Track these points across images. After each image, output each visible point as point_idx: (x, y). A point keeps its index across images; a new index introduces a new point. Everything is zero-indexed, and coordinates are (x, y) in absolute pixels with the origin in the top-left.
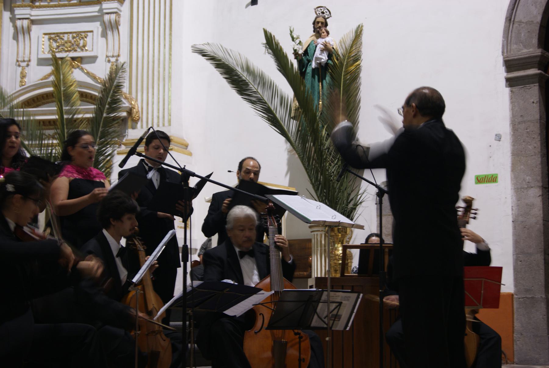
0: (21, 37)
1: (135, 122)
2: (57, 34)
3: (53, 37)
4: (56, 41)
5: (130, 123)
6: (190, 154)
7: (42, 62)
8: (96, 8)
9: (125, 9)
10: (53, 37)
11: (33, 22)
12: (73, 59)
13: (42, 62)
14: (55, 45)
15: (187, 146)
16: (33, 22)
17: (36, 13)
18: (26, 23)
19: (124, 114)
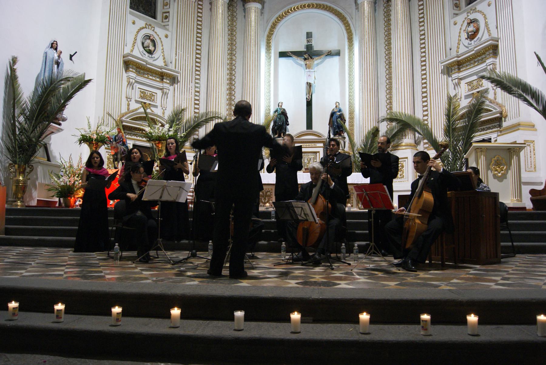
0: (456, 88)
1: (505, 118)
2: (470, 82)
3: (469, 84)
4: (470, 85)
5: (503, 119)
6: (536, 130)
7: (467, 97)
8: (485, 64)
9: (497, 60)
10: (469, 84)
11: (461, 79)
12: (478, 92)
13: (467, 97)
14: (470, 87)
15: (534, 126)
16: (461, 79)
17: (461, 75)
18: (456, 80)
19: (498, 115)
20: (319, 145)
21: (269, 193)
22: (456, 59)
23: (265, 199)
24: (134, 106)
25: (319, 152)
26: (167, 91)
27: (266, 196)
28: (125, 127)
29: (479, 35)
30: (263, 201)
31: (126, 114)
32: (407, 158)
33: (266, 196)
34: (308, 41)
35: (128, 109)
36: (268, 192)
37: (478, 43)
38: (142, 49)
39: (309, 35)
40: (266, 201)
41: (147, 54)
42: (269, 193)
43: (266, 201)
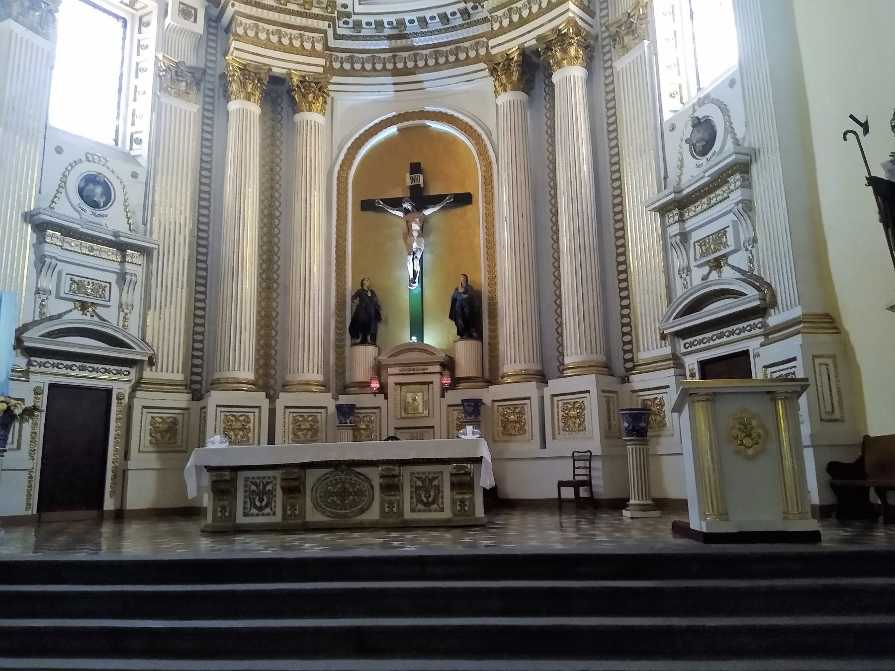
20: (431, 369)
21: (269, 487)
22: (672, 196)
23: (261, 501)
24: (55, 307)
25: (432, 383)
26: (134, 278)
27: (264, 492)
28: (30, 352)
29: (716, 147)
30: (258, 504)
31: (35, 323)
32: (588, 392)
33: (264, 492)
34: (413, 179)
35: (41, 314)
36: (268, 483)
37: (715, 160)
38: (77, 200)
39: (415, 168)
40: (264, 503)
41: (89, 210)
42: (269, 487)
43: (264, 503)
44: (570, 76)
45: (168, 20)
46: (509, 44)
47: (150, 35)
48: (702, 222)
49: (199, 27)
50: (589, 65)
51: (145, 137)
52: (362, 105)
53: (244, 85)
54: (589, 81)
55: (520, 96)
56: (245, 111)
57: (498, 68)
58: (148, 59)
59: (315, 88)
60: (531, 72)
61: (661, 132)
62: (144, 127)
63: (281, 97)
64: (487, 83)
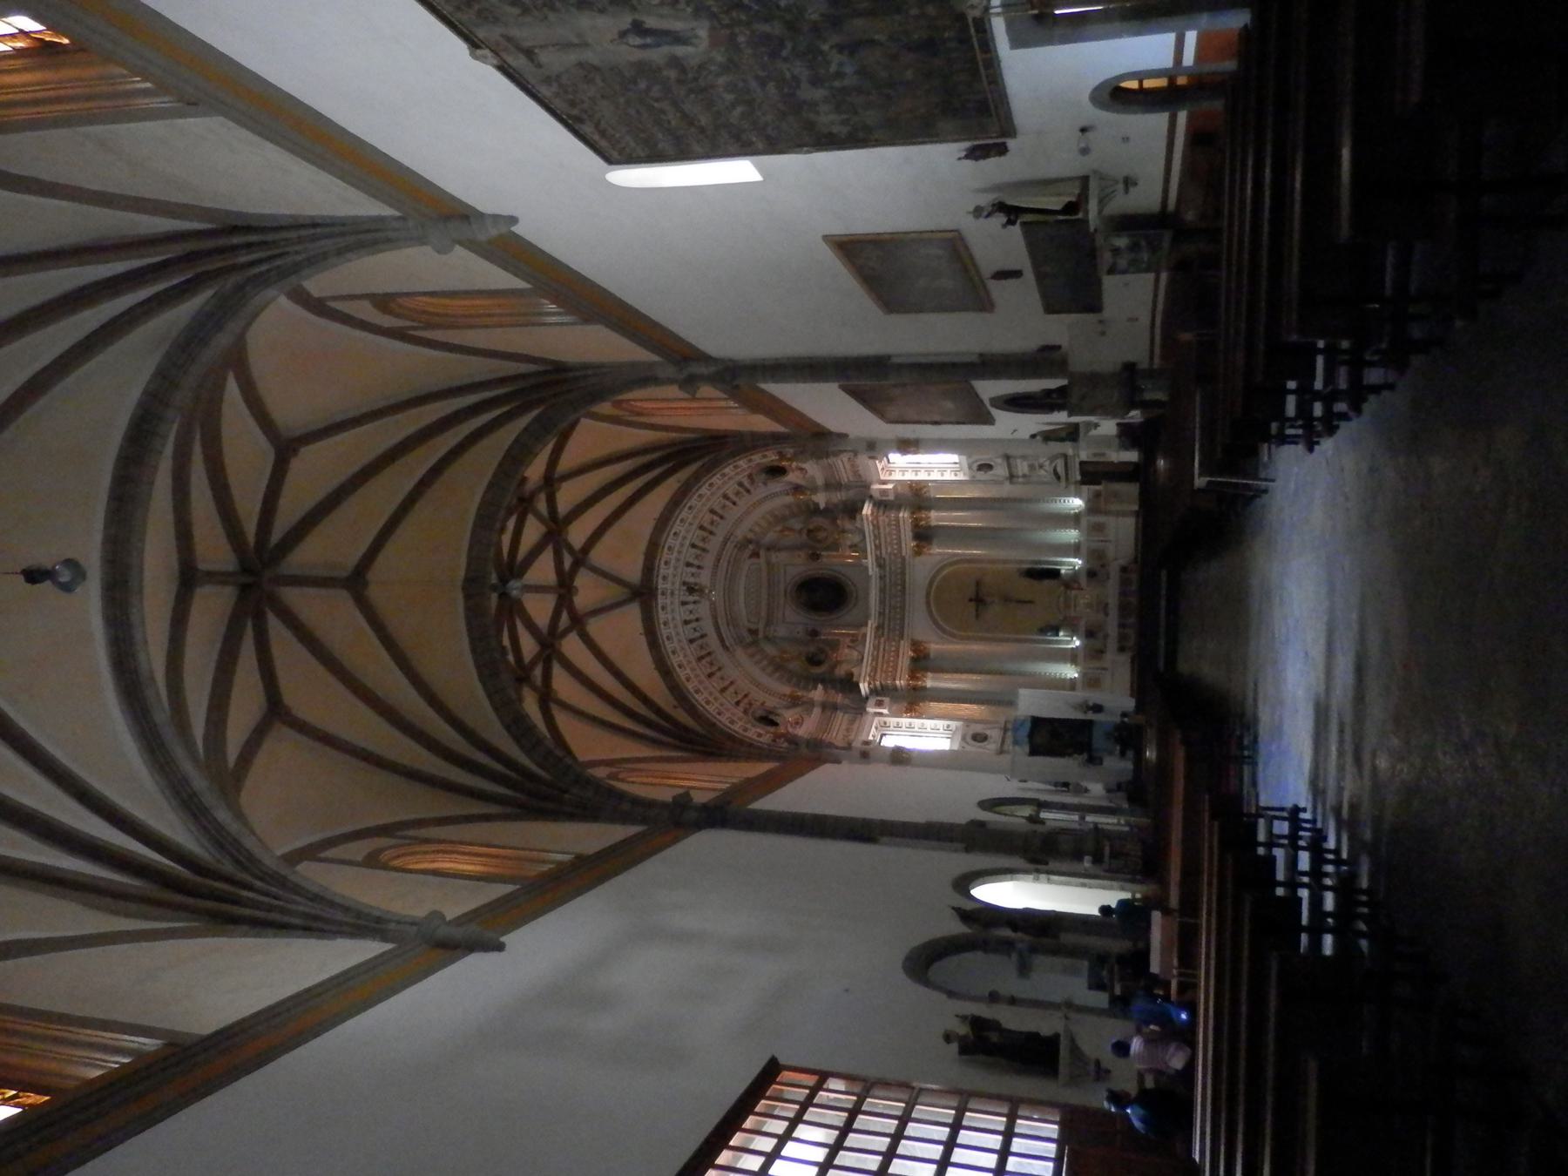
44: (936, 517)
45: (885, 711)
46: (909, 543)
47: (893, 721)
48: (1022, 467)
49: (887, 700)
50: (929, 509)
51: (947, 723)
52: (920, 626)
53: (918, 679)
54: (939, 509)
55: (935, 541)
56: (930, 682)
57: (918, 552)
58: (905, 721)
59: (916, 645)
60: (924, 535)
61: (973, 481)
62: (941, 724)
63: (921, 662)
64: (923, 558)
